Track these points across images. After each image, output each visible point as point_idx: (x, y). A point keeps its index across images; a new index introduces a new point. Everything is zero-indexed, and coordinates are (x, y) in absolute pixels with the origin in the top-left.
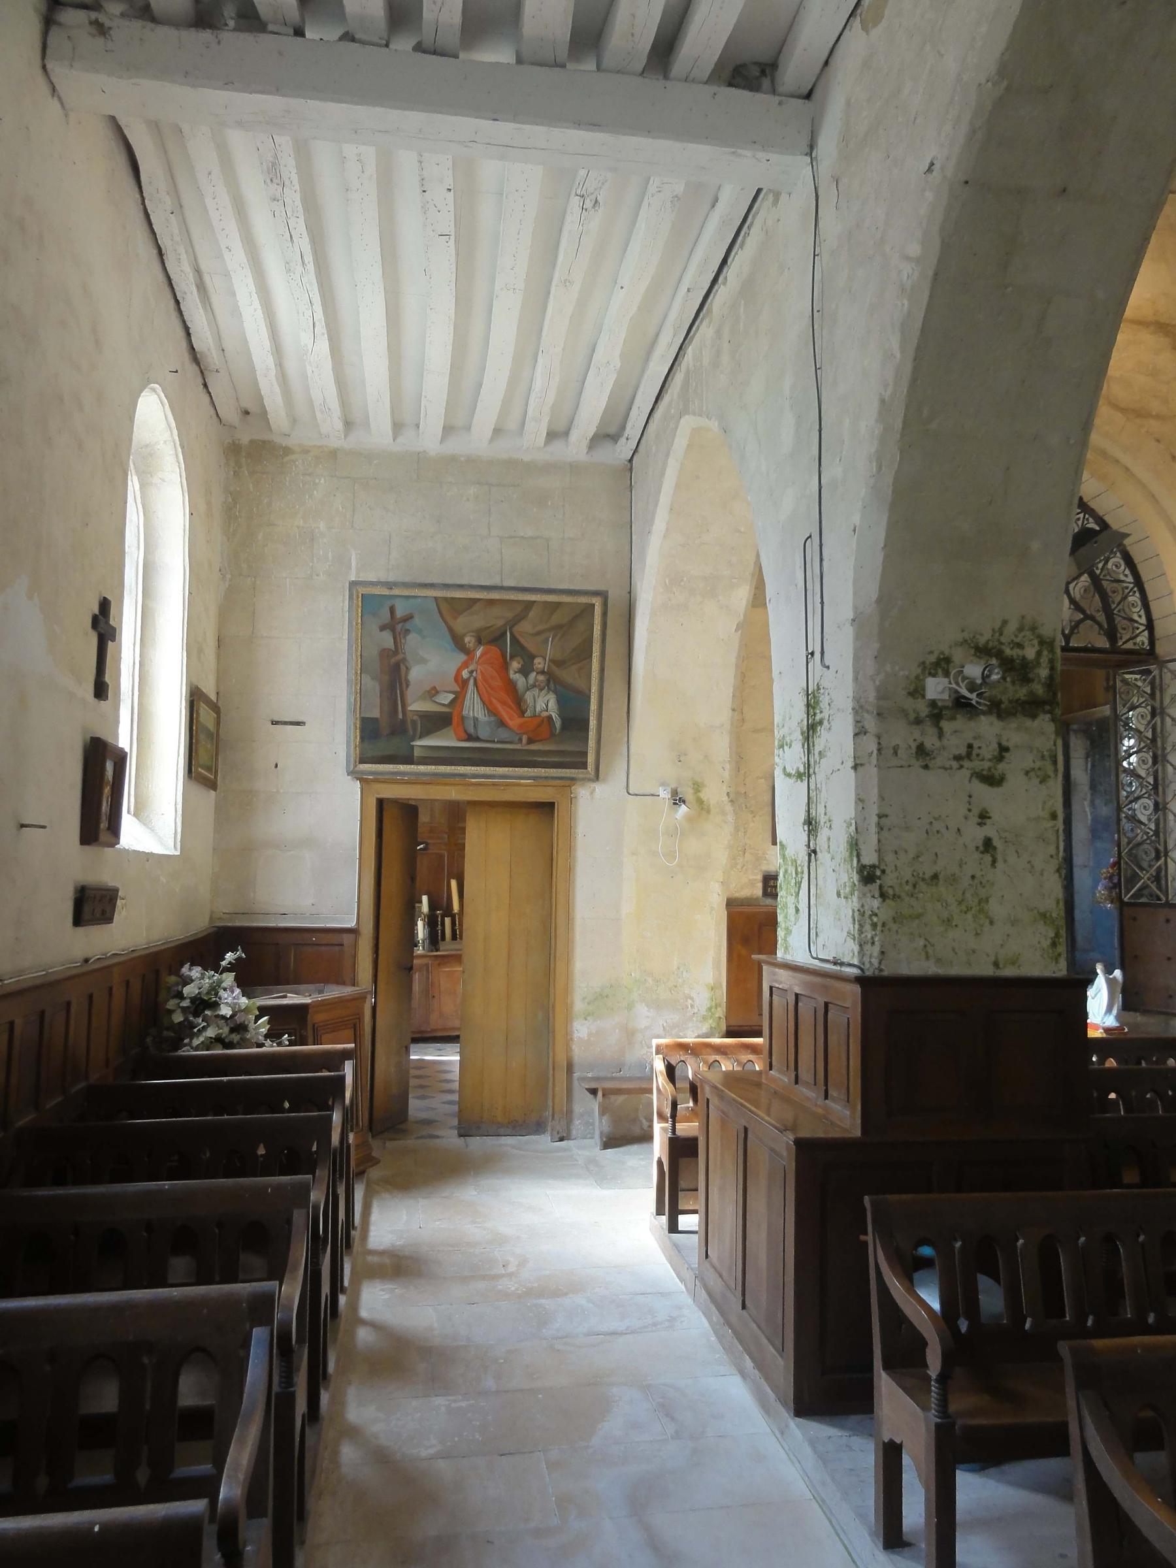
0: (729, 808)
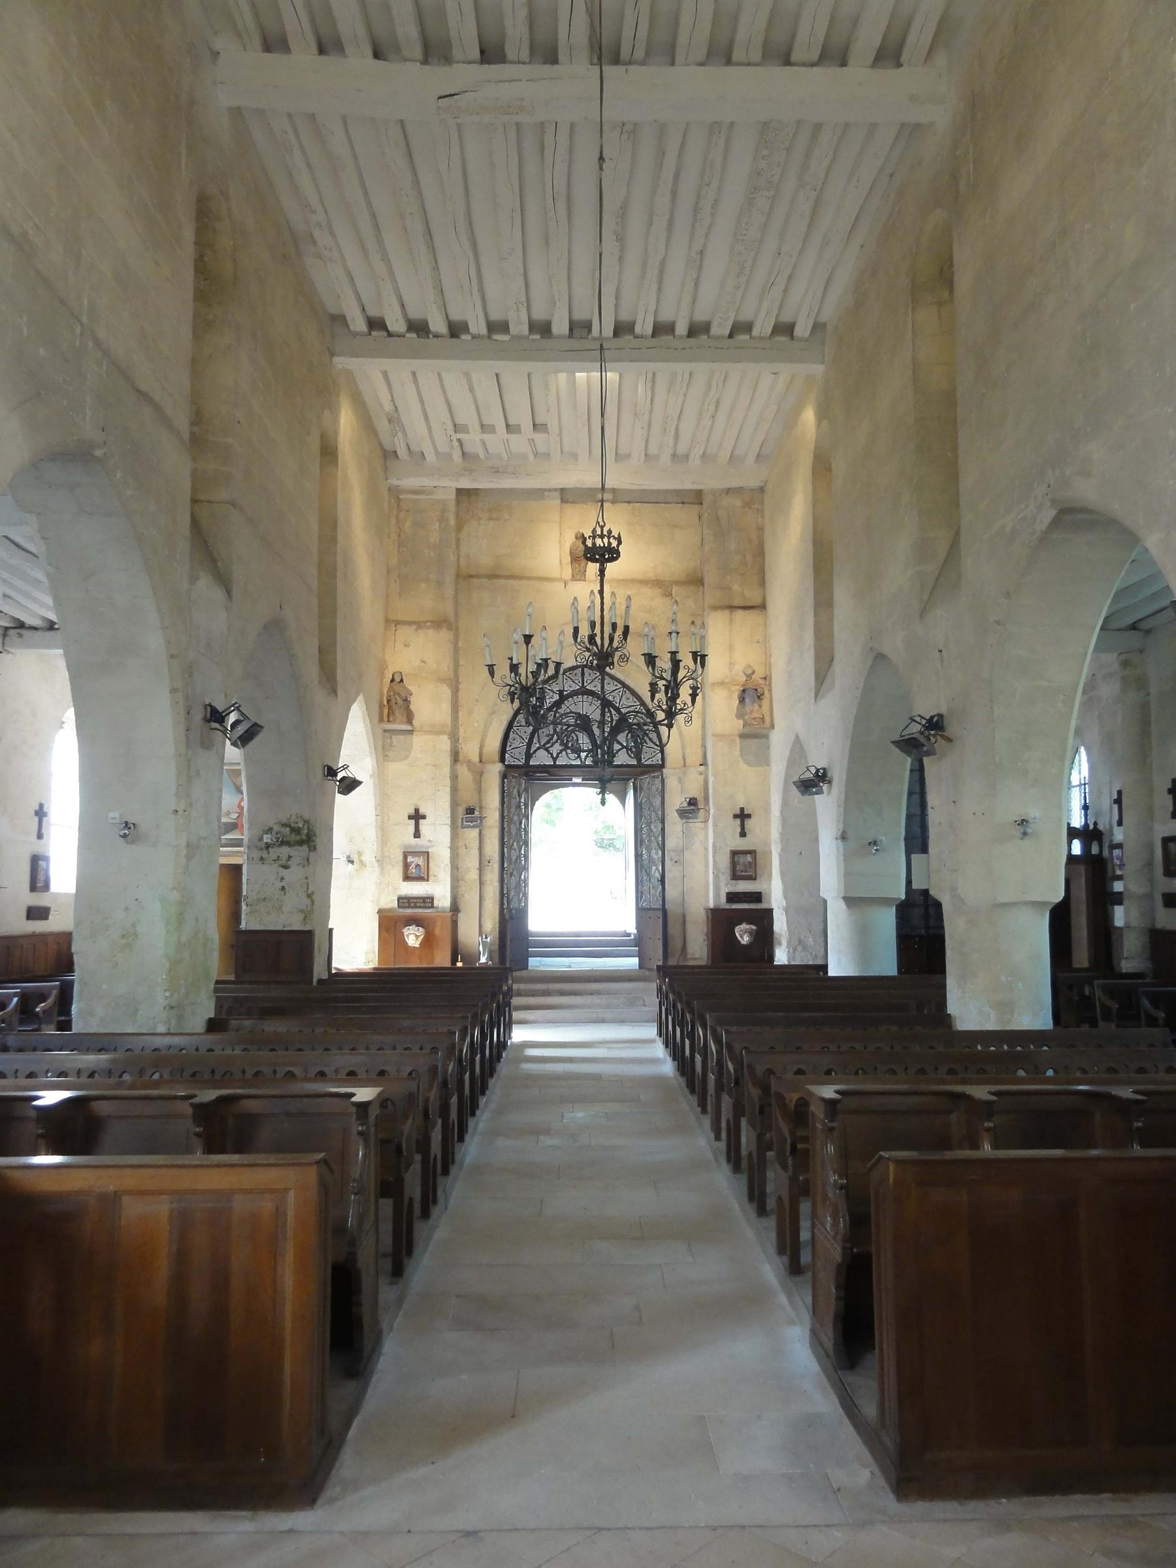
0: (376, 864)
